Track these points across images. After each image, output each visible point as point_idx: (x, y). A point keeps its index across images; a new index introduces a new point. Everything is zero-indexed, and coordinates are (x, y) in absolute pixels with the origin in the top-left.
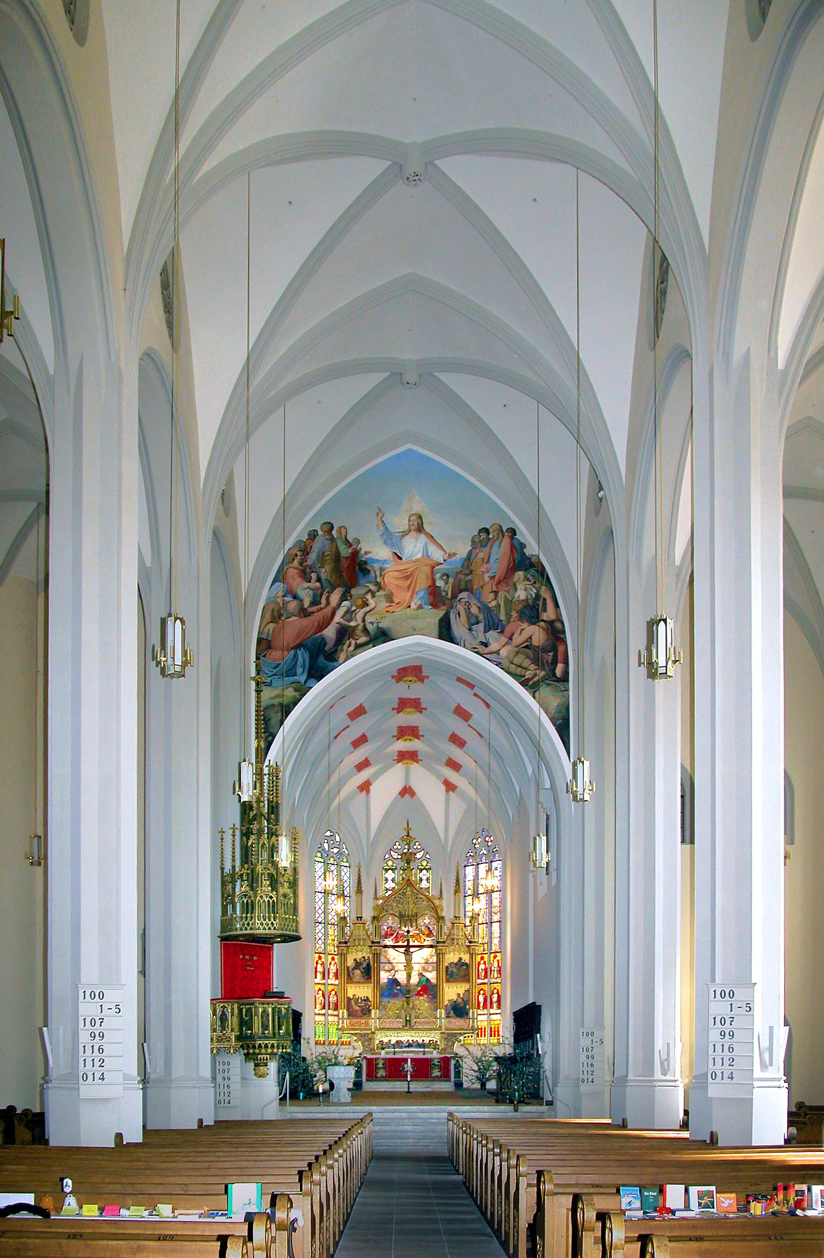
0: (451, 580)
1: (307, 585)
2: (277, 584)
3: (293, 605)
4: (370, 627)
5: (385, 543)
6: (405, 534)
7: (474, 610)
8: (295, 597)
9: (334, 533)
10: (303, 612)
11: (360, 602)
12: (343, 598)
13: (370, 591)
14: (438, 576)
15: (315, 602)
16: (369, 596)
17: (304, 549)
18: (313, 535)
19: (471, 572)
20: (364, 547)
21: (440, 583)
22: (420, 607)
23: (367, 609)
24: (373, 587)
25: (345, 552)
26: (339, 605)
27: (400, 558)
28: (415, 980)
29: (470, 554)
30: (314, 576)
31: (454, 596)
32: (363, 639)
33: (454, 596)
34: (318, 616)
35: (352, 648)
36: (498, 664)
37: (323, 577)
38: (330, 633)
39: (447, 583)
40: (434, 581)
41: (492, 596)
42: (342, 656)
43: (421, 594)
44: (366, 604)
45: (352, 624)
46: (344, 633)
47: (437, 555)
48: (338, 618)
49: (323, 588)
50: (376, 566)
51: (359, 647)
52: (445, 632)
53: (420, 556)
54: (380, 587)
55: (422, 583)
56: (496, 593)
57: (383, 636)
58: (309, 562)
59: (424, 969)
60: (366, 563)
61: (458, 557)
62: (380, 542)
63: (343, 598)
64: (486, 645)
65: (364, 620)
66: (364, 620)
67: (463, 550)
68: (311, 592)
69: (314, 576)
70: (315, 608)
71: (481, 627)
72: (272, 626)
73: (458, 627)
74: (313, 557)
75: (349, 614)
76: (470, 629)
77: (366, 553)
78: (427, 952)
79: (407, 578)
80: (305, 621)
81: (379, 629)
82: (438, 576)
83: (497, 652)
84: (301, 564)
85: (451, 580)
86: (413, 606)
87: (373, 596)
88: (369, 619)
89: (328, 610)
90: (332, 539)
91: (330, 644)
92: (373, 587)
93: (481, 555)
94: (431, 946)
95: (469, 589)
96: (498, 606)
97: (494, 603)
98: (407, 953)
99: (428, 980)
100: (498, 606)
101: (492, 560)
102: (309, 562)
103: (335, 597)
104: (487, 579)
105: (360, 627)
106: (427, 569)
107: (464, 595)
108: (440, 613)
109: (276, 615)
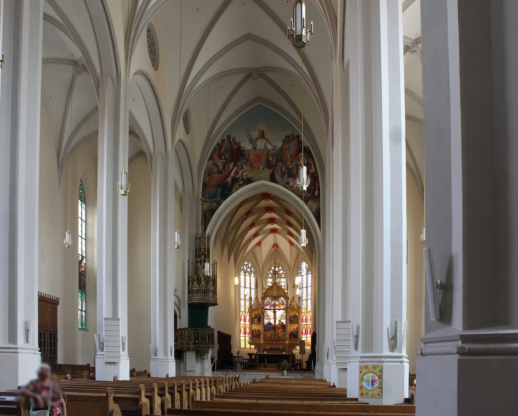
0: (275, 157)
1: (220, 161)
2: (210, 161)
3: (216, 169)
4: (244, 178)
5: (250, 143)
6: (257, 139)
7: (284, 169)
8: (217, 166)
9: (231, 139)
10: (219, 172)
11: (240, 167)
12: (234, 166)
13: (244, 163)
14: (270, 156)
15: (224, 168)
16: (244, 165)
17: (219, 146)
18: (223, 141)
19: (283, 154)
20: (242, 145)
21: (271, 159)
22: (263, 169)
23: (243, 170)
24: (245, 161)
25: (235, 147)
26: (233, 169)
27: (256, 149)
29: (282, 146)
30: (223, 157)
31: (276, 164)
32: (241, 183)
33: (276, 164)
34: (225, 173)
35: (237, 186)
36: (293, 192)
37: (227, 157)
38: (229, 180)
39: (273, 158)
40: (268, 158)
41: (290, 163)
42: (234, 190)
43: (263, 164)
44: (243, 168)
45: (238, 176)
46: (235, 180)
47: (270, 147)
48: (232, 174)
49: (227, 162)
50: (247, 152)
51: (241, 186)
52: (273, 179)
53: (263, 148)
54: (248, 161)
55: (264, 159)
56: (292, 162)
57: (249, 181)
58: (222, 152)
59: (281, 319)
60: (243, 151)
61: (277, 148)
62: (248, 143)
63: (234, 166)
64: (288, 183)
65: (242, 175)
66: (242, 175)
67: (279, 145)
68: (222, 164)
69: (223, 157)
70: (224, 170)
71: (286, 176)
72: (208, 178)
73: (278, 177)
74: (223, 149)
75: (237, 172)
76: (282, 177)
77: (243, 147)
78: (282, 312)
79: (258, 157)
80: (220, 176)
81: (247, 178)
82: (270, 156)
83: (293, 187)
84: (219, 152)
85: (275, 157)
86: (261, 168)
87: (246, 165)
88: (244, 174)
89: (229, 170)
90: (230, 142)
91: (229, 185)
92: (245, 161)
93: (286, 147)
94: (283, 309)
95: (282, 161)
96: (293, 167)
97: (291, 166)
98: (275, 312)
100: (293, 167)
101: (290, 149)
102: (222, 152)
103: (231, 166)
104: (288, 155)
105: (241, 178)
106: (266, 153)
107: (280, 163)
108: (271, 171)
109: (209, 173)
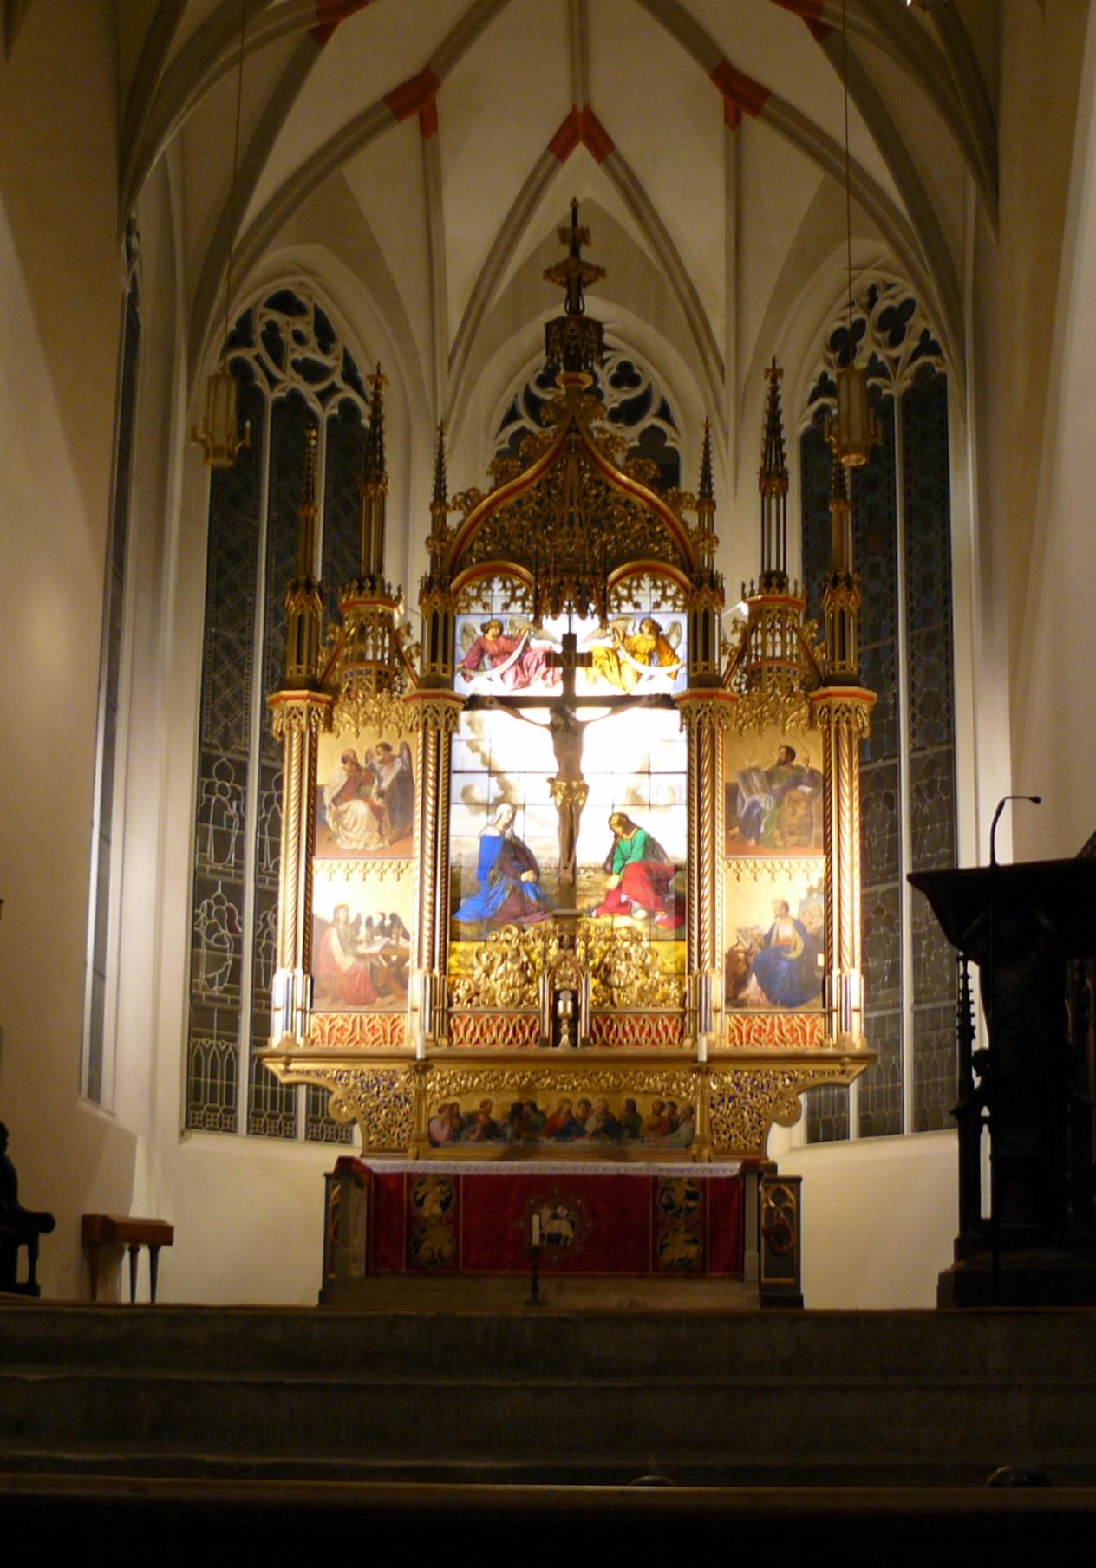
28: (593, 846)
99: (651, 846)
